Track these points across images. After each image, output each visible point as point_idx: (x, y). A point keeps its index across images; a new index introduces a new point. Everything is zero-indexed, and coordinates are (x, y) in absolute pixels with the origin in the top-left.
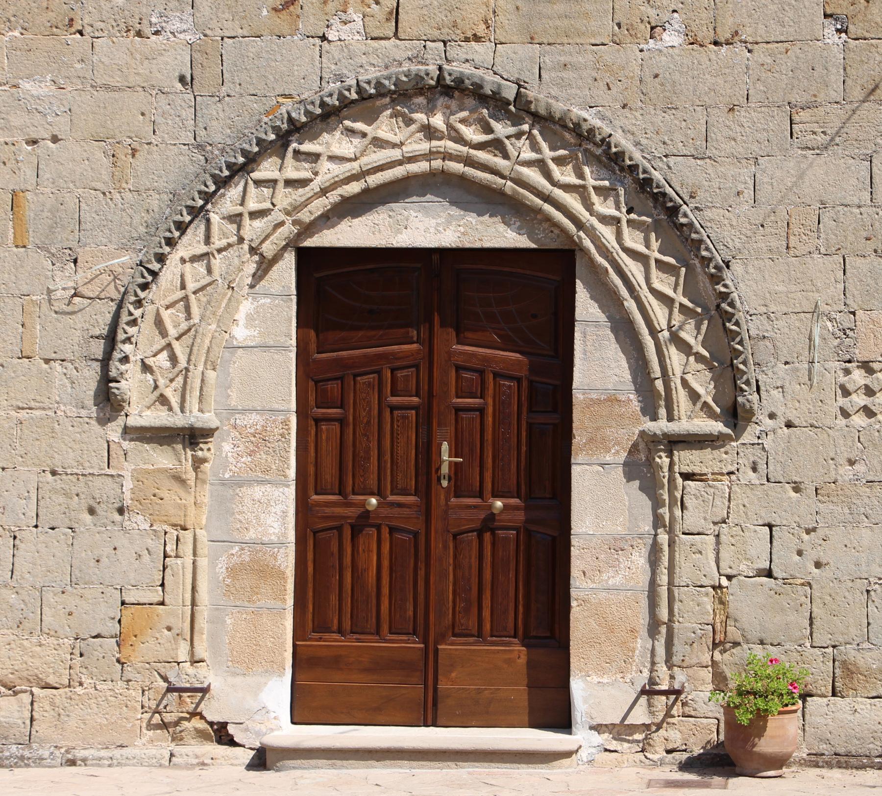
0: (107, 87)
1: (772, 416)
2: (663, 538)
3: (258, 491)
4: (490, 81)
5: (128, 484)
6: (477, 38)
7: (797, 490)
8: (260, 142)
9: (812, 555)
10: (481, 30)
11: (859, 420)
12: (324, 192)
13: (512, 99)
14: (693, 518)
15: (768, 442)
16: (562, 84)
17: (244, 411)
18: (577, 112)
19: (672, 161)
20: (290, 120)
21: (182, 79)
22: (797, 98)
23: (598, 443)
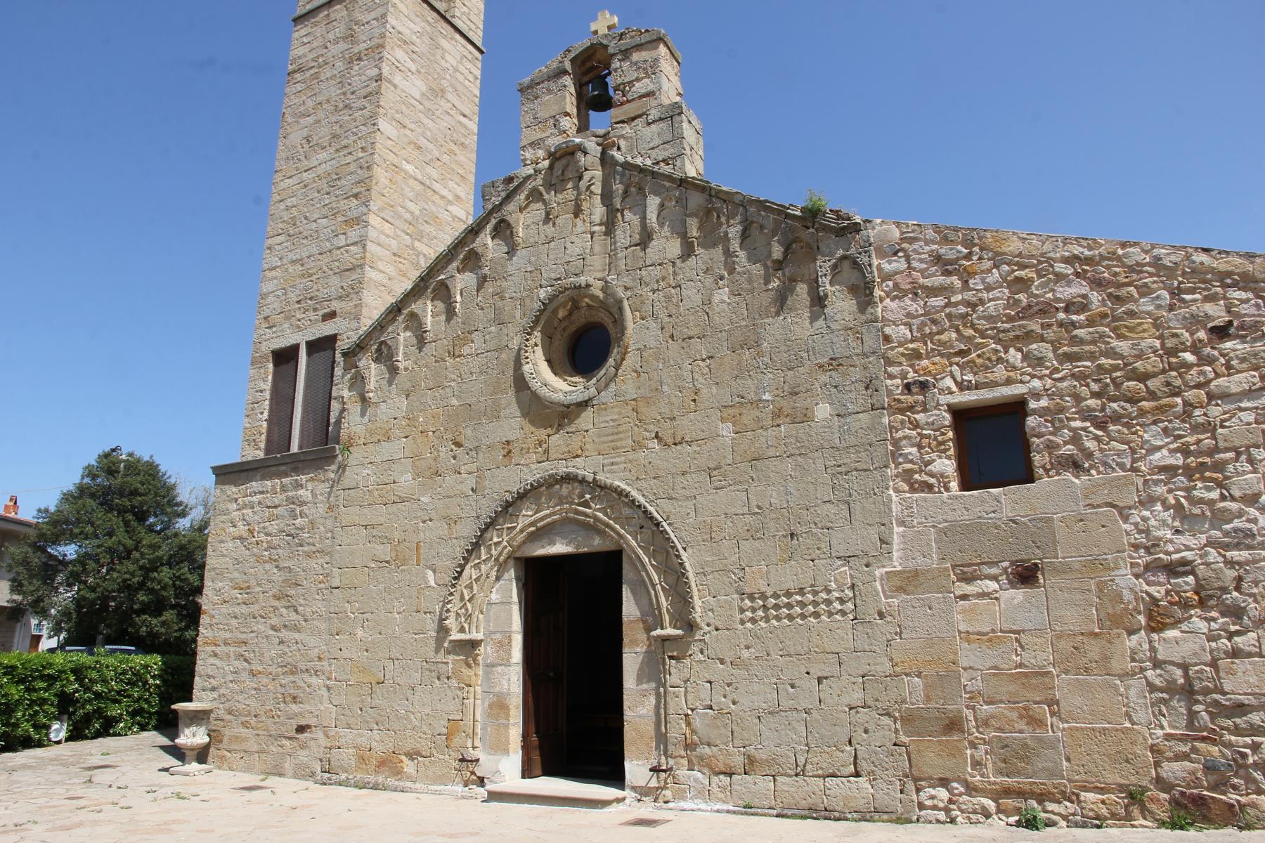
0: (449, 497)
1: (708, 625)
2: (662, 690)
3: (499, 669)
4: (581, 472)
5: (451, 666)
6: (578, 456)
8: (496, 512)
9: (730, 697)
10: (579, 452)
11: (749, 625)
12: (522, 531)
13: (591, 480)
14: (673, 679)
15: (707, 638)
16: (611, 472)
17: (494, 633)
18: (617, 483)
19: (658, 501)
21: (472, 490)
22: (712, 466)
23: (634, 642)
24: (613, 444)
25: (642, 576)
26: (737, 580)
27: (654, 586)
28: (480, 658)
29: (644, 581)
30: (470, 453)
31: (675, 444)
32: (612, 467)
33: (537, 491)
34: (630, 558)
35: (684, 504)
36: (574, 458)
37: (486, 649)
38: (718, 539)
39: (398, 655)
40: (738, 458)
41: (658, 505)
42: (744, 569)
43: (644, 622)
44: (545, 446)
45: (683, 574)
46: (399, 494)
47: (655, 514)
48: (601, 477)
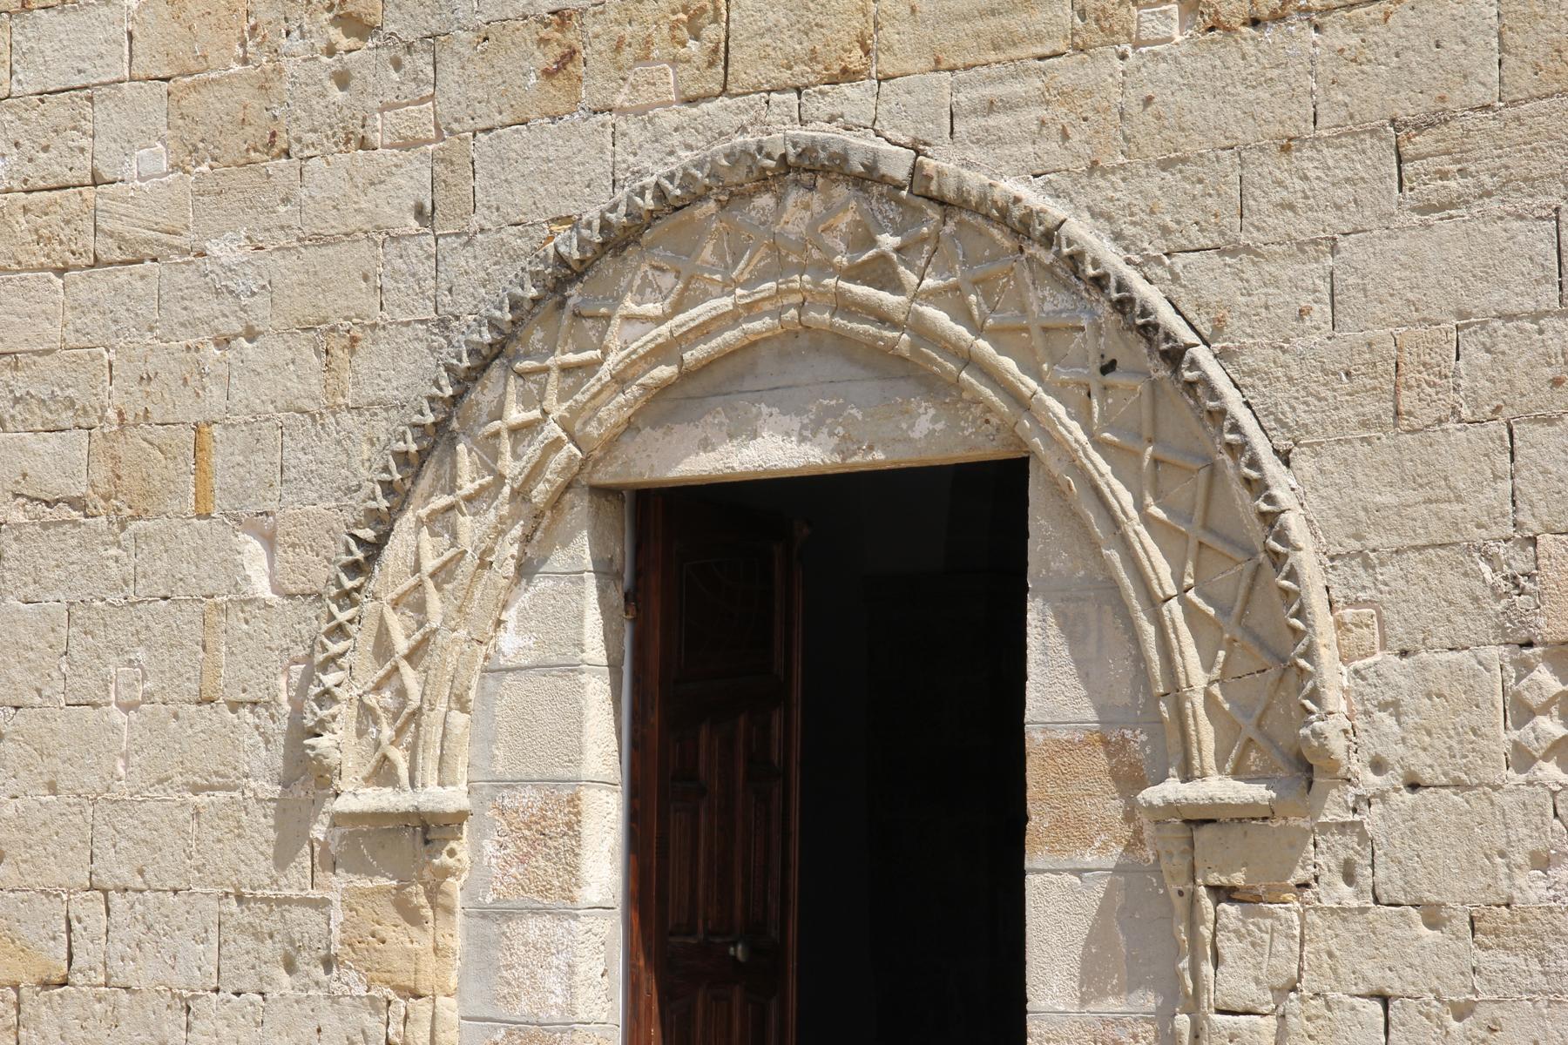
0: (320, 240)
1: (1378, 766)
2: (1183, 1021)
3: (533, 928)
4: (861, 144)
5: (338, 915)
6: (848, 75)
7: (1433, 923)
10: (855, 58)
12: (621, 380)
13: (901, 174)
15: (1371, 818)
16: (985, 140)
17: (512, 785)
18: (1009, 186)
19: (1179, 261)
20: (561, 260)
21: (419, 212)
22: (1406, 109)
23: (1074, 830)
24: (993, 22)
25: (1105, 565)
26: (1505, 586)
27: (1154, 604)
28: (453, 885)
29: (1114, 586)
30: (406, 60)
31: (1255, 22)
32: (992, 121)
33: (681, 216)
34: (1058, 491)
35: (1290, 271)
36: (833, 82)
37: (477, 850)
38: (1426, 415)
39: (126, 875)
40: (1525, 80)
41: (1175, 278)
42: (1533, 541)
43: (1114, 749)
44: (712, 32)
45: (1277, 559)
46: (118, 226)
47: (1166, 315)
48: (943, 162)
